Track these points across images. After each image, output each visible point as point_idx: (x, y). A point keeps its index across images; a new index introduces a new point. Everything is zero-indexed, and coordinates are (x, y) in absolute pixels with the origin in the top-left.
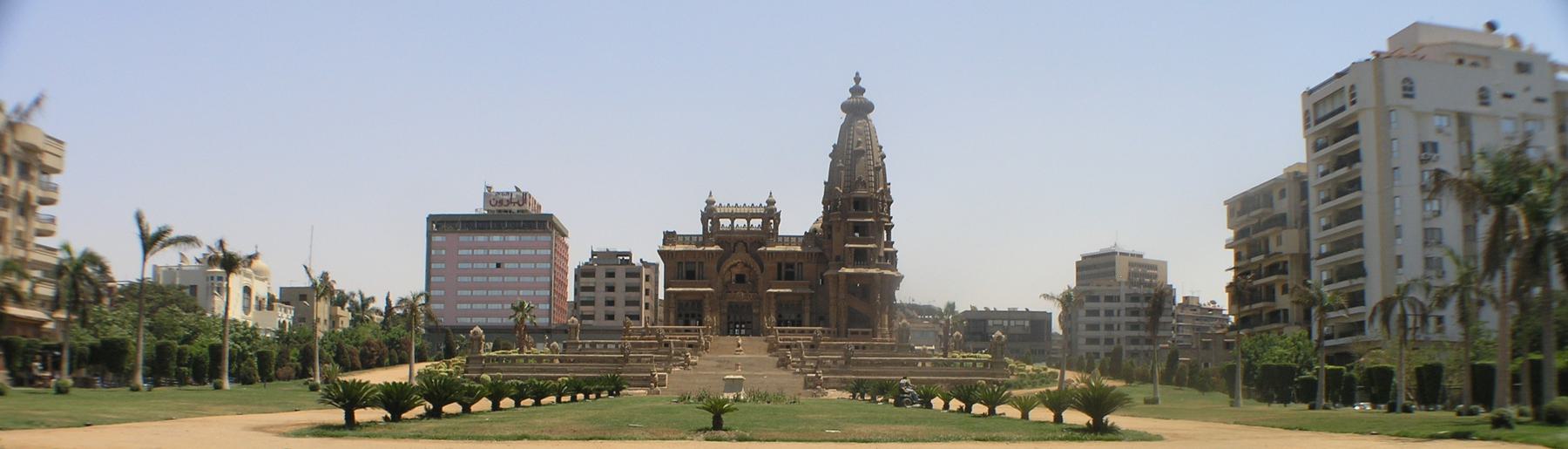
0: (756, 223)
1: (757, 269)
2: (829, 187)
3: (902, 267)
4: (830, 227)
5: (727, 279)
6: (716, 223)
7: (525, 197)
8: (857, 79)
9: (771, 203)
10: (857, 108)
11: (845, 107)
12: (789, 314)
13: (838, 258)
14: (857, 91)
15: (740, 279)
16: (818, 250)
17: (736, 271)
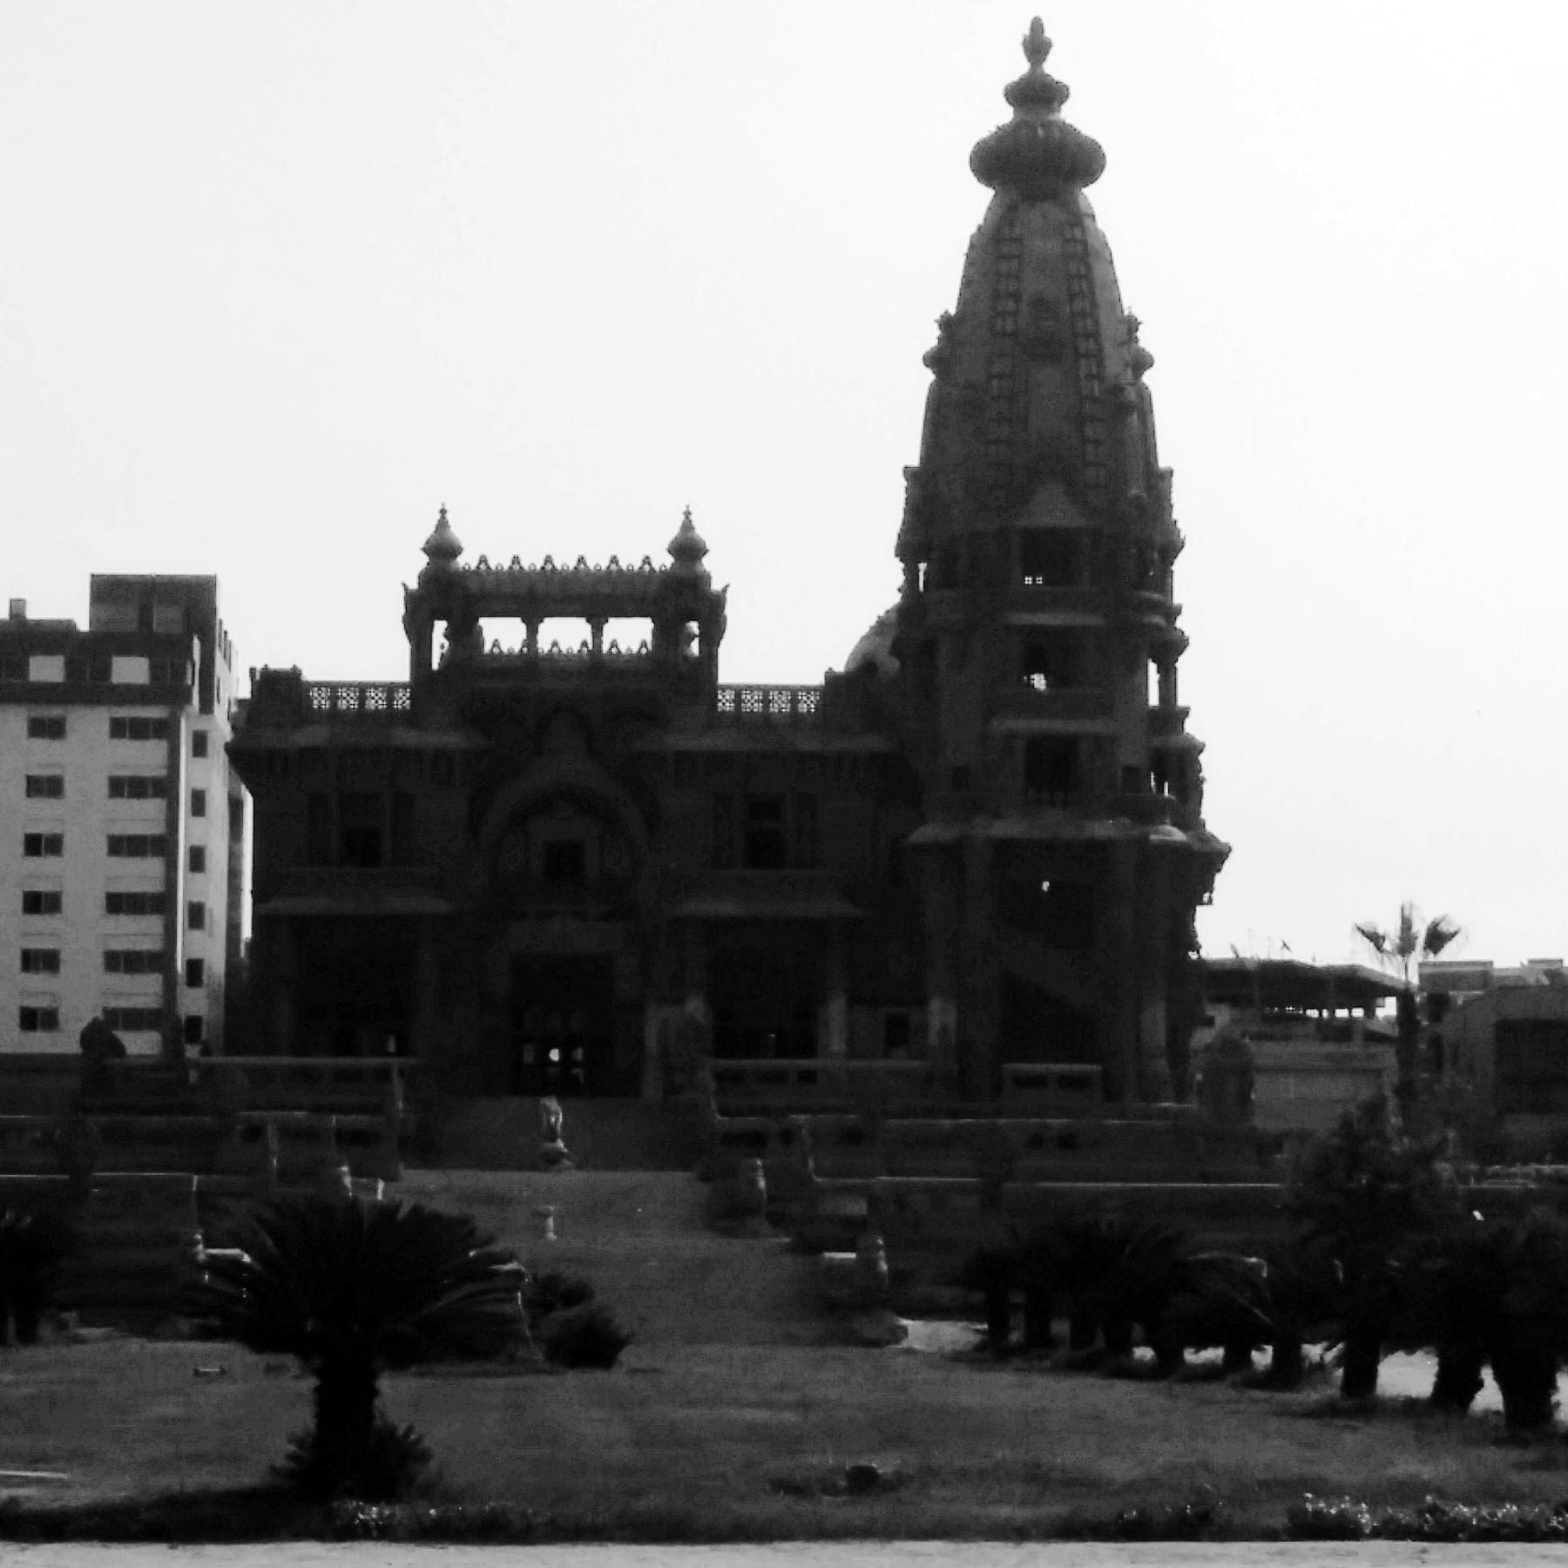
0: (630, 634)
3: (1219, 813)
4: (928, 649)
6: (465, 634)
8: (1037, 47)
9: (688, 549)
10: (1037, 165)
11: (992, 162)
14: (1036, 94)
15: (564, 862)
16: (874, 743)
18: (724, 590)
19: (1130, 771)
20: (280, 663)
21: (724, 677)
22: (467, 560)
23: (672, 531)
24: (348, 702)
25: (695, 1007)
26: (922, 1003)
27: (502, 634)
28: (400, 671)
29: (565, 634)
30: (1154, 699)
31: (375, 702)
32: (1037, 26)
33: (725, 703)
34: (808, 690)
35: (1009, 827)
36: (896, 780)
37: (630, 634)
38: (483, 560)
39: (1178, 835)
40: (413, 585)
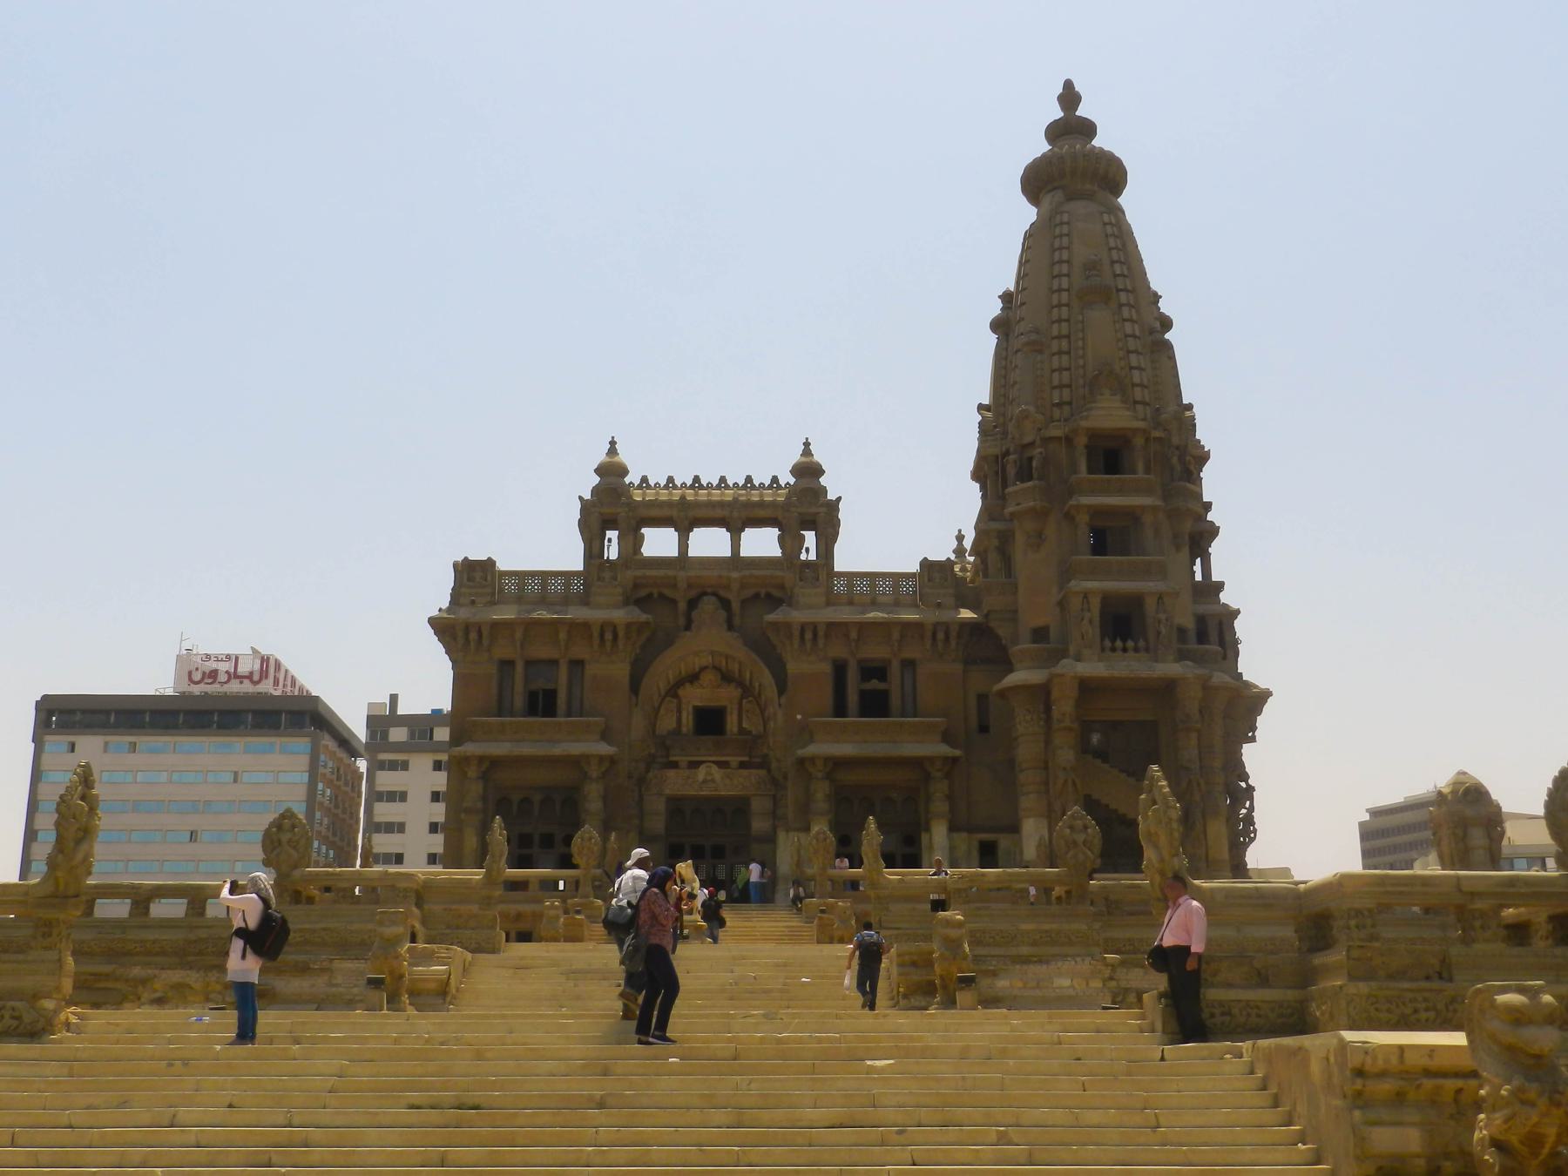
0: (762, 543)
1: (766, 679)
2: (997, 423)
5: (667, 723)
7: (268, 666)
8: (1069, 97)
9: (808, 471)
10: (1075, 178)
12: (885, 811)
13: (1040, 634)
14: (1071, 128)
15: (710, 721)
17: (696, 696)
18: (839, 499)
19: (1182, 631)
22: (633, 478)
23: (795, 456)
24: (533, 587)
25: (820, 827)
26: (1014, 829)
27: (659, 542)
28: (577, 564)
29: (709, 543)
30: (1198, 577)
31: (556, 586)
32: (1068, 85)
33: (839, 586)
35: (1093, 668)
36: (984, 646)
37: (762, 543)
38: (644, 479)
39: (1227, 679)
40: (587, 496)
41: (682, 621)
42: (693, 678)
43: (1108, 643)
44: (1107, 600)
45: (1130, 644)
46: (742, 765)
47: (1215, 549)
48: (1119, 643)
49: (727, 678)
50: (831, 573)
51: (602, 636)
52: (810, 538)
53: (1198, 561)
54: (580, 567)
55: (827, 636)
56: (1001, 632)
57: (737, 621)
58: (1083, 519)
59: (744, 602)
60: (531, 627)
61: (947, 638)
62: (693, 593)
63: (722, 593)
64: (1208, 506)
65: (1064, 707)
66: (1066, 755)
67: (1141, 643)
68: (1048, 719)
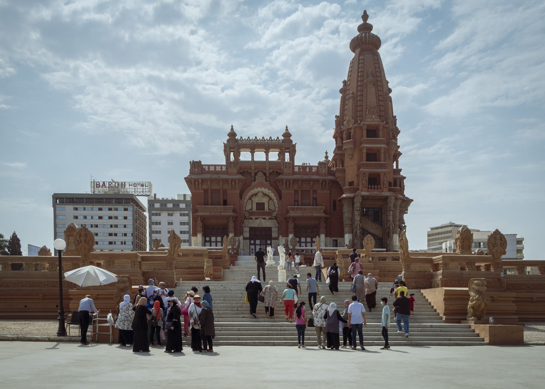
6: (237, 155)
13: (351, 184)
17: (256, 200)
20: (197, 160)
21: (295, 164)
26: (343, 236)
28: (224, 163)
30: (395, 167)
31: (218, 169)
33: (296, 169)
34: (315, 166)
37: (274, 156)
41: (253, 179)
42: (256, 195)
43: (370, 186)
44: (370, 174)
45: (376, 187)
46: (270, 219)
47: (400, 159)
48: (373, 186)
49: (265, 195)
50: (293, 166)
51: (232, 182)
52: (287, 155)
53: (395, 162)
54: (225, 164)
55: (293, 183)
56: (340, 183)
57: (268, 179)
58: (365, 151)
59: (270, 174)
60: (212, 180)
61: (326, 183)
62: (256, 171)
63: (264, 171)
64: (399, 147)
65: (357, 205)
66: (357, 218)
67: (379, 186)
68: (353, 207)
